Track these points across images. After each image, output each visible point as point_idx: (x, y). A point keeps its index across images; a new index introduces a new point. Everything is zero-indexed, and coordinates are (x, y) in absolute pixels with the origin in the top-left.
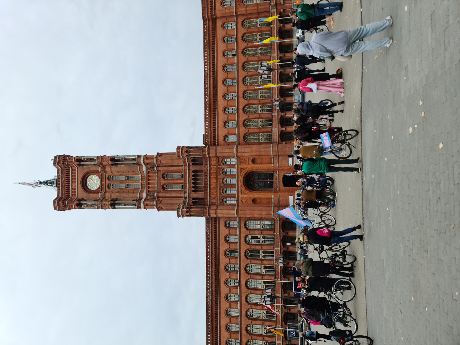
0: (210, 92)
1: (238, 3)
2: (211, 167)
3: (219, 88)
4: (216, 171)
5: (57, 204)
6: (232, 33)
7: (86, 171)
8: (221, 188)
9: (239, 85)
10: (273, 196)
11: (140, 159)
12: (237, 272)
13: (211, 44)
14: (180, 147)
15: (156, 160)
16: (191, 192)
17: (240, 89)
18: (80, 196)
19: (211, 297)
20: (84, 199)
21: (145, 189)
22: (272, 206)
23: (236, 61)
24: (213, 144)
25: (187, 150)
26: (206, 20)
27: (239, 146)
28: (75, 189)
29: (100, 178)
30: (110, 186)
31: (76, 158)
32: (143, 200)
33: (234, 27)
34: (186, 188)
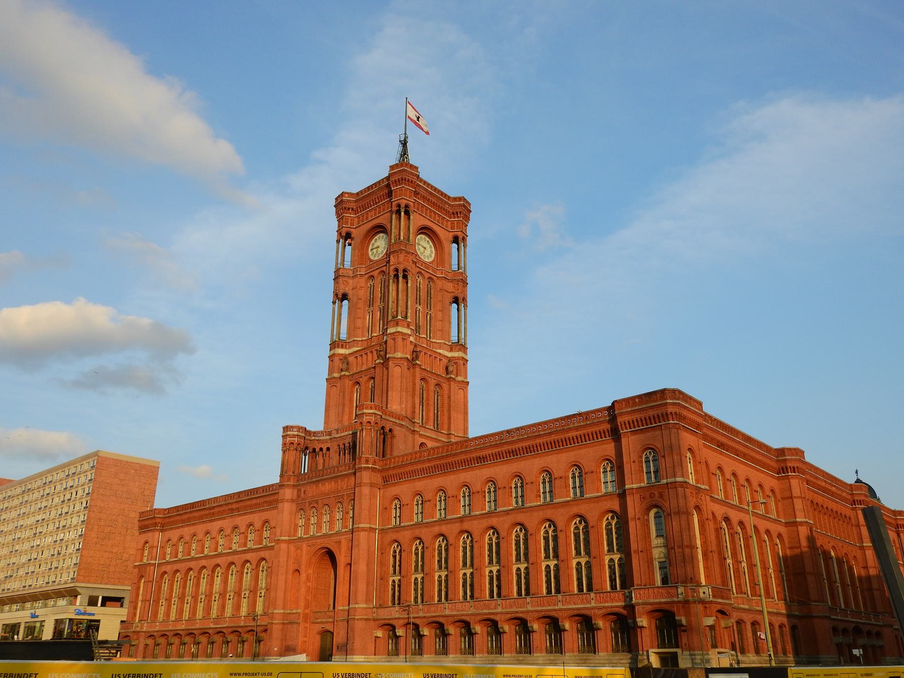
0: (470, 452)
2: (346, 479)
3: (477, 472)
4: (339, 489)
6: (588, 486)
8: (318, 504)
9: (484, 518)
10: (299, 611)
11: (394, 327)
12: (231, 548)
17: (476, 522)
18: (354, 233)
19: (208, 506)
22: (284, 609)
28: (367, 218)
29: (383, 256)
33: (604, 491)
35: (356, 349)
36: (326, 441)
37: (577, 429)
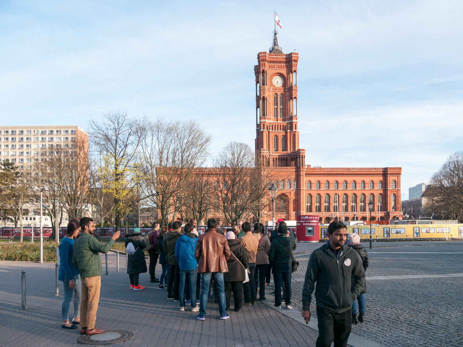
1: (393, 191)
5: (264, 55)
7: (286, 76)
13: (369, 173)
14: (305, 151)
15: (294, 131)
16: (273, 157)
18: (268, 72)
20: (267, 75)
21: (273, 122)
23: (357, 189)
24: (306, 173)
25: (303, 157)
26: (385, 170)
27: (304, 191)
30: (275, 95)
31: (296, 69)
32: (267, 121)
34: (276, 153)
35: (272, 122)
36: (268, 155)
37: (374, 172)
